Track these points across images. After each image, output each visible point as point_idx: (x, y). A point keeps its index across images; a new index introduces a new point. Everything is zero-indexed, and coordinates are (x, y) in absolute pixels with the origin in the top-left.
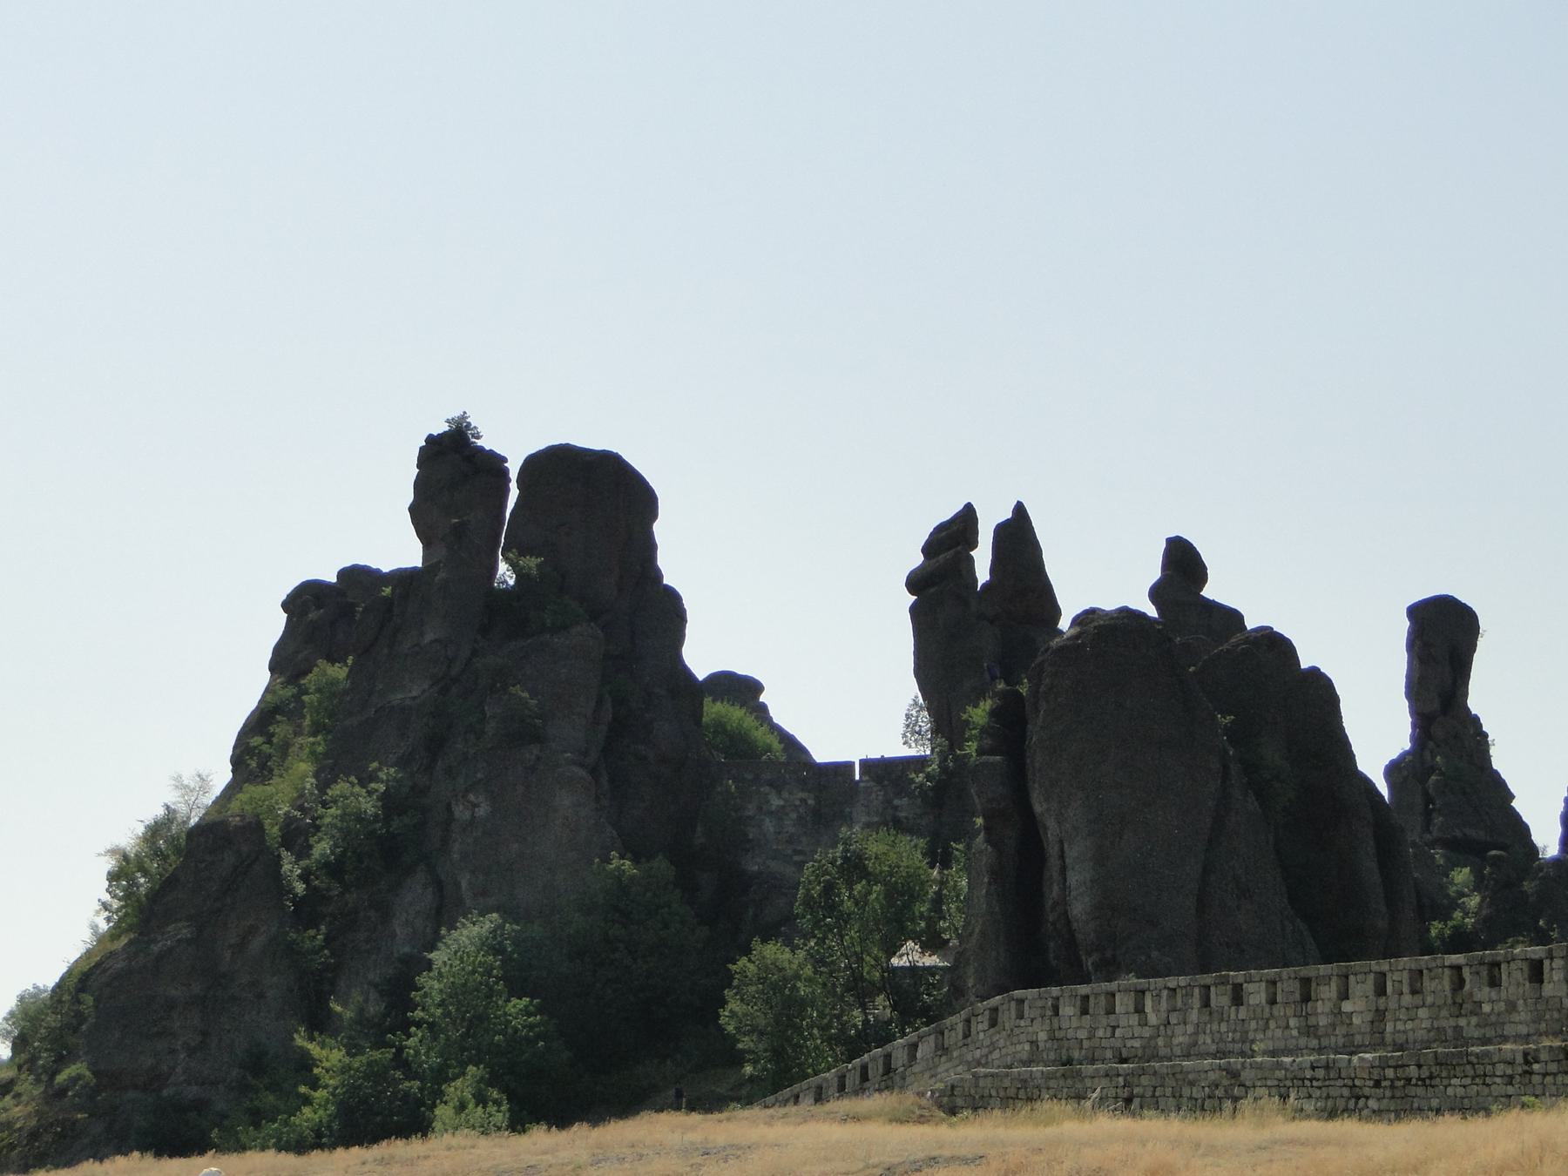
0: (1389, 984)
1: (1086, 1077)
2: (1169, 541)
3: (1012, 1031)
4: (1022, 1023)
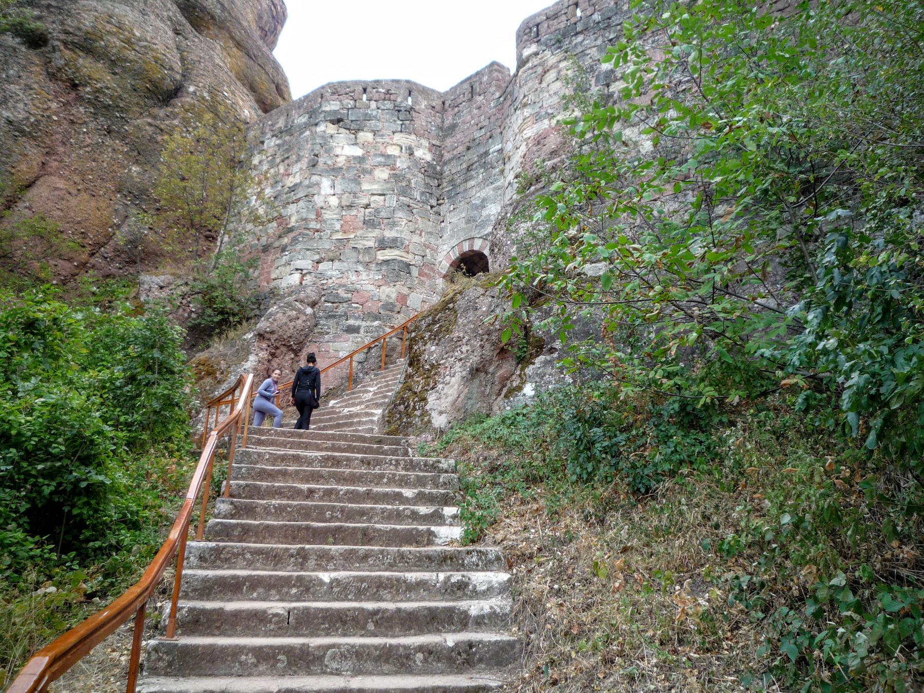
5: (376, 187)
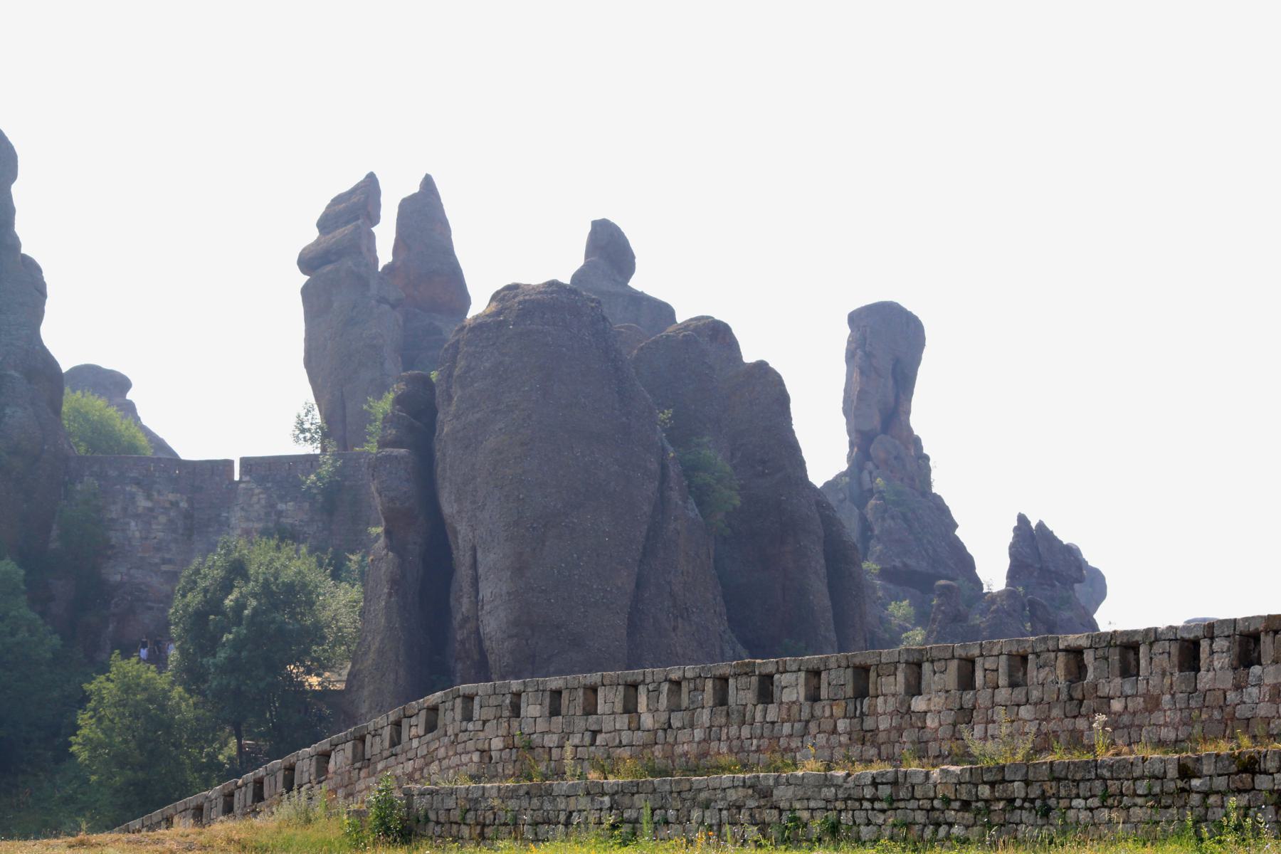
0: (979, 675)
1: (558, 796)
2: (596, 224)
3: (456, 735)
4: (470, 726)
5: (160, 527)
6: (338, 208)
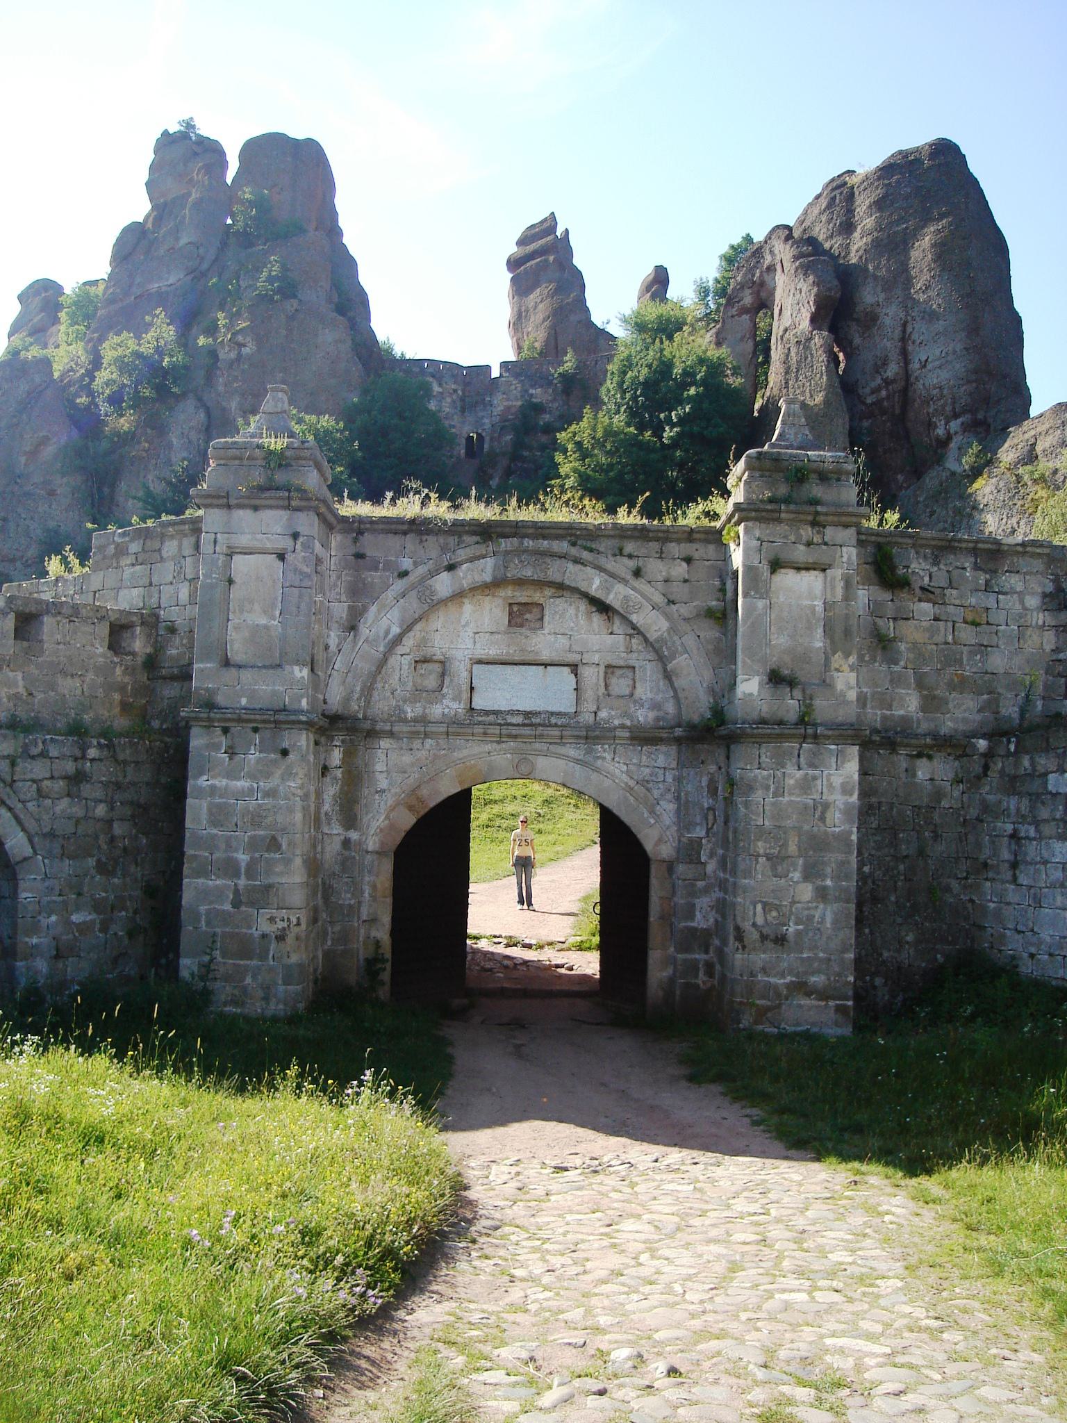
6: (533, 232)
